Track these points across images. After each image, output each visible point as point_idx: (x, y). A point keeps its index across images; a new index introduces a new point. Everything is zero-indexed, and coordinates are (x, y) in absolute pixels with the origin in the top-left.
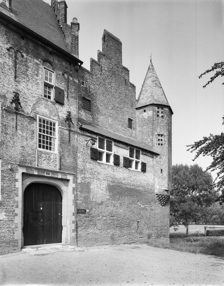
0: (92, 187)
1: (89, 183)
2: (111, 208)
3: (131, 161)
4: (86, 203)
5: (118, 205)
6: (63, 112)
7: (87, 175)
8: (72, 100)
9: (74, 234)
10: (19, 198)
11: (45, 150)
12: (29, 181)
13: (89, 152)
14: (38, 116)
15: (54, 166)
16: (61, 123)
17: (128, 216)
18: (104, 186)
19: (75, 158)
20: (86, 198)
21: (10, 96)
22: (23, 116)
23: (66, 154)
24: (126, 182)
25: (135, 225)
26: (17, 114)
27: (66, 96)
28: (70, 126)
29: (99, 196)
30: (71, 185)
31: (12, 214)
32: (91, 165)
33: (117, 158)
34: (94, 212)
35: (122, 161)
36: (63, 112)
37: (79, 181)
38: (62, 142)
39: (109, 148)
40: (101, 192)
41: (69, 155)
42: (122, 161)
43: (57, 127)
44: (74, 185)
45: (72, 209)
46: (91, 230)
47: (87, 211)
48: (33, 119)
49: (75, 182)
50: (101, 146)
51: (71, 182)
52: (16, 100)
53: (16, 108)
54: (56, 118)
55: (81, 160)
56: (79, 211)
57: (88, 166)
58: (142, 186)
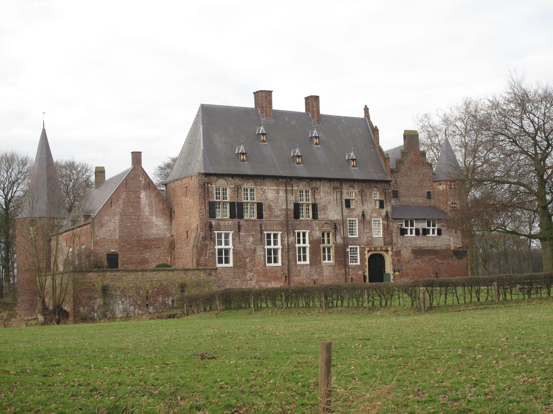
0: (402, 252)
1: (400, 251)
5: (420, 262)
13: (399, 231)
14: (372, 219)
18: (410, 251)
20: (399, 260)
27: (385, 202)
30: (390, 253)
33: (417, 231)
35: (421, 232)
37: (394, 250)
40: (407, 255)
41: (388, 236)
44: (391, 253)
49: (392, 251)
52: (363, 215)
55: (395, 237)
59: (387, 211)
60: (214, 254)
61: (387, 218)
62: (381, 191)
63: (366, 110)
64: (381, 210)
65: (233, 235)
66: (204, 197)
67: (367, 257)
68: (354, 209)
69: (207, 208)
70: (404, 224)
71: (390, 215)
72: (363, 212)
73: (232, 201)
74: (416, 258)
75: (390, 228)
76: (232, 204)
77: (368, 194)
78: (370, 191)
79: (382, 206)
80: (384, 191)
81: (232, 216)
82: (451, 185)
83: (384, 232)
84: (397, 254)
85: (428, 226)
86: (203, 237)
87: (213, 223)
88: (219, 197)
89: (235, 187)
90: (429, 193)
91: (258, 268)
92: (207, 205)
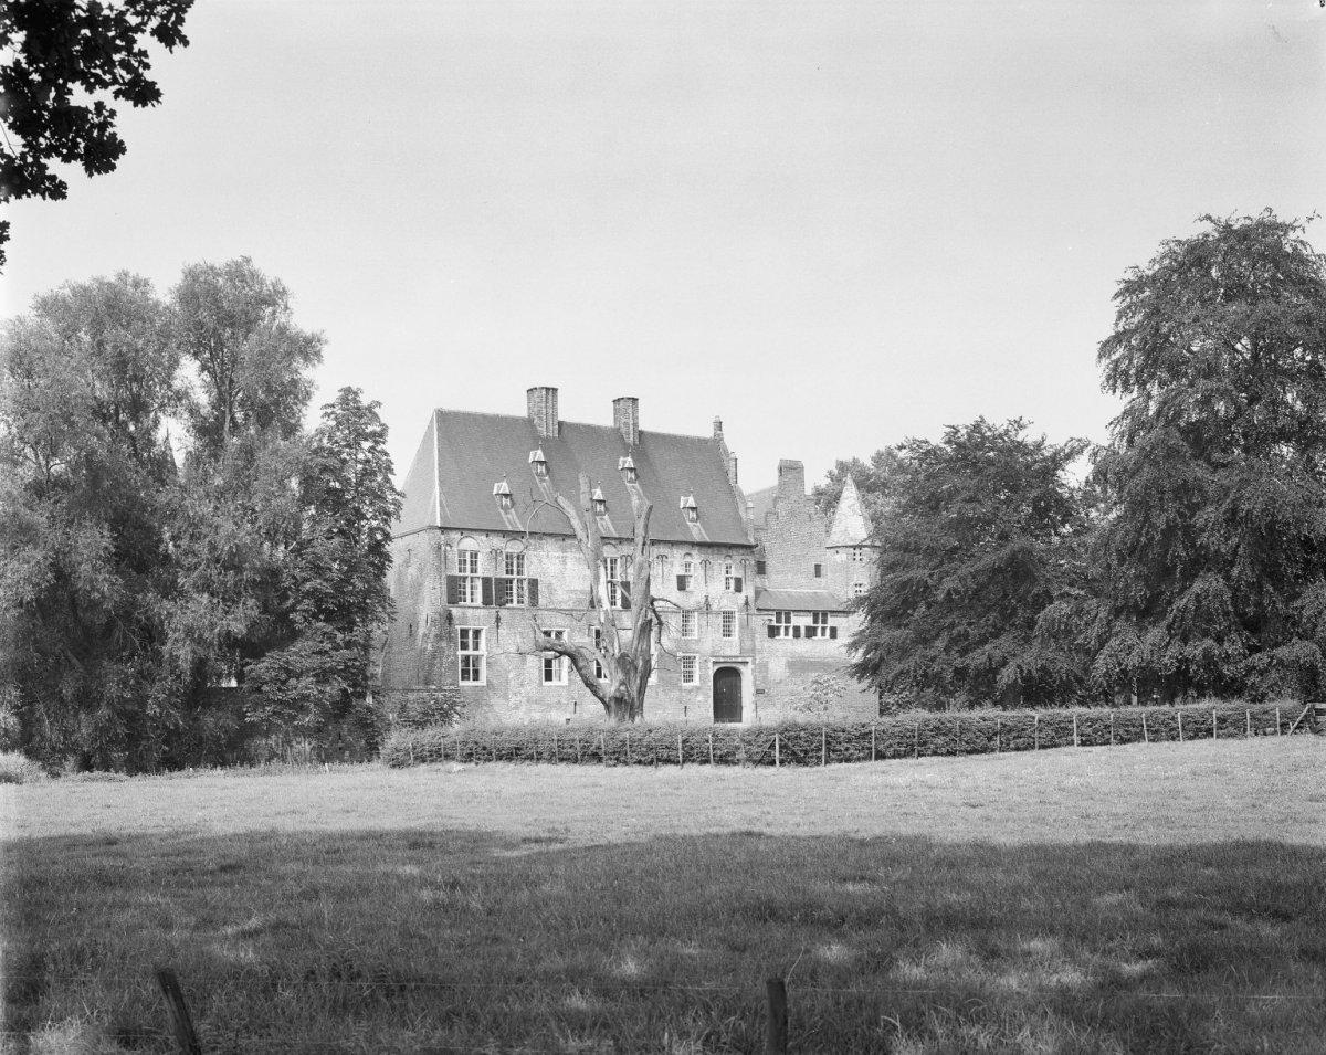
0: (771, 666)
2: (790, 687)
3: (815, 629)
6: (741, 598)
12: (716, 668)
13: (766, 630)
15: (736, 652)
16: (740, 611)
19: (753, 640)
20: (765, 678)
21: (703, 600)
30: (750, 666)
32: (768, 643)
33: (797, 629)
35: (803, 631)
36: (741, 598)
38: (742, 627)
39: (788, 620)
42: (803, 631)
43: (737, 615)
45: (752, 690)
49: (754, 663)
50: (778, 621)
51: (750, 664)
56: (759, 692)
58: (832, 657)
60: (454, 663)
63: (719, 425)
65: (488, 632)
66: (439, 568)
67: (711, 673)
68: (691, 592)
69: (445, 588)
70: (774, 618)
72: (707, 597)
73: (486, 575)
75: (752, 625)
76: (486, 581)
79: (738, 589)
81: (487, 602)
83: (740, 631)
84: (763, 667)
86: (436, 636)
87: (455, 611)
88: (512, 570)
90: (818, 567)
91: (529, 688)
92: (444, 581)
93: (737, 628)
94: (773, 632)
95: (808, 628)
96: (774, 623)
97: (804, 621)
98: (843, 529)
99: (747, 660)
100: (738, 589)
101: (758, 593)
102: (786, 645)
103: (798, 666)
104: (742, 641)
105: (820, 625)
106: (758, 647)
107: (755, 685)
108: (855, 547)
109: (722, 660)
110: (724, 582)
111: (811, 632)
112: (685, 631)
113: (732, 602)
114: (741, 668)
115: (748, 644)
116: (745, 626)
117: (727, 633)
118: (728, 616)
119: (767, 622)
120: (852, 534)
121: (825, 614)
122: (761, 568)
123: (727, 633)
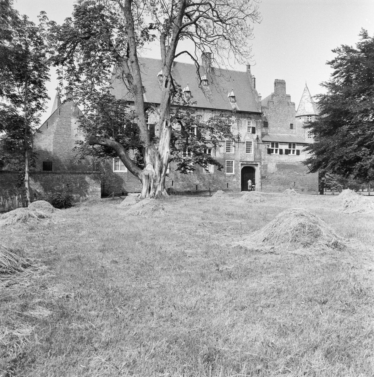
0: (268, 166)
1: (267, 165)
2: (278, 175)
3: (290, 151)
4: (265, 173)
6: (255, 136)
7: (266, 161)
8: (258, 130)
9: (260, 187)
10: (240, 173)
11: (248, 153)
12: (242, 167)
13: (267, 150)
16: (254, 141)
17: (288, 179)
20: (266, 171)
22: (241, 142)
23: (257, 153)
24: (287, 161)
25: (293, 183)
26: (239, 142)
28: (258, 141)
29: (272, 170)
30: (259, 166)
31: (237, 179)
32: (267, 156)
33: (281, 151)
34: (270, 178)
35: (284, 152)
36: (255, 136)
38: (255, 149)
39: (277, 146)
40: (272, 168)
42: (284, 152)
43: (253, 143)
44: (260, 166)
45: (260, 177)
46: (268, 186)
47: (266, 177)
48: (244, 143)
49: (261, 165)
50: (273, 146)
51: (259, 165)
53: (239, 141)
54: (252, 140)
56: (263, 178)
57: (266, 157)
59: (258, 136)
61: (258, 141)
62: (254, 120)
64: (253, 134)
70: (270, 145)
71: (260, 139)
74: (279, 170)
77: (243, 122)
78: (245, 120)
79: (254, 132)
80: (256, 120)
82: (308, 119)
83: (254, 150)
84: (265, 167)
85: (289, 148)
89: (131, 112)
90: (291, 125)
93: (253, 149)
94: (270, 151)
95: (286, 150)
96: (270, 147)
97: (285, 147)
98: (303, 108)
99: (258, 163)
100: (254, 132)
101: (263, 135)
102: (276, 157)
103: (281, 167)
104: (255, 155)
105: (292, 149)
106: (263, 157)
107: (261, 174)
108: (308, 116)
109: (245, 163)
110: (247, 129)
111: (288, 152)
112: (228, 150)
113: (251, 138)
114: (256, 168)
115: (258, 156)
116: (256, 149)
117: (248, 151)
118: (249, 144)
119: (267, 147)
120: (307, 110)
121: (294, 144)
122: (266, 124)
123: (248, 151)
